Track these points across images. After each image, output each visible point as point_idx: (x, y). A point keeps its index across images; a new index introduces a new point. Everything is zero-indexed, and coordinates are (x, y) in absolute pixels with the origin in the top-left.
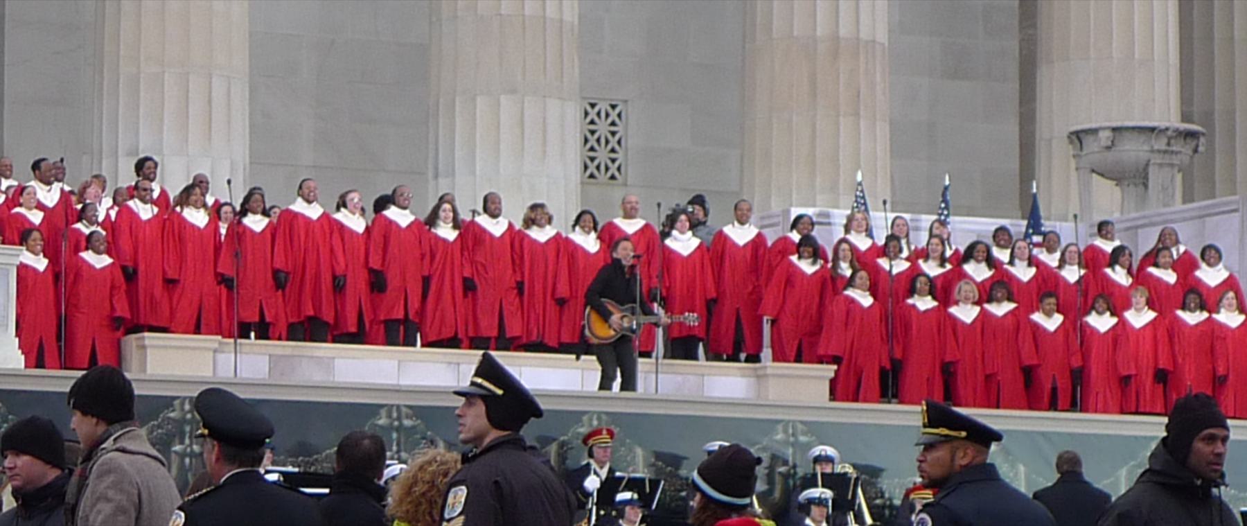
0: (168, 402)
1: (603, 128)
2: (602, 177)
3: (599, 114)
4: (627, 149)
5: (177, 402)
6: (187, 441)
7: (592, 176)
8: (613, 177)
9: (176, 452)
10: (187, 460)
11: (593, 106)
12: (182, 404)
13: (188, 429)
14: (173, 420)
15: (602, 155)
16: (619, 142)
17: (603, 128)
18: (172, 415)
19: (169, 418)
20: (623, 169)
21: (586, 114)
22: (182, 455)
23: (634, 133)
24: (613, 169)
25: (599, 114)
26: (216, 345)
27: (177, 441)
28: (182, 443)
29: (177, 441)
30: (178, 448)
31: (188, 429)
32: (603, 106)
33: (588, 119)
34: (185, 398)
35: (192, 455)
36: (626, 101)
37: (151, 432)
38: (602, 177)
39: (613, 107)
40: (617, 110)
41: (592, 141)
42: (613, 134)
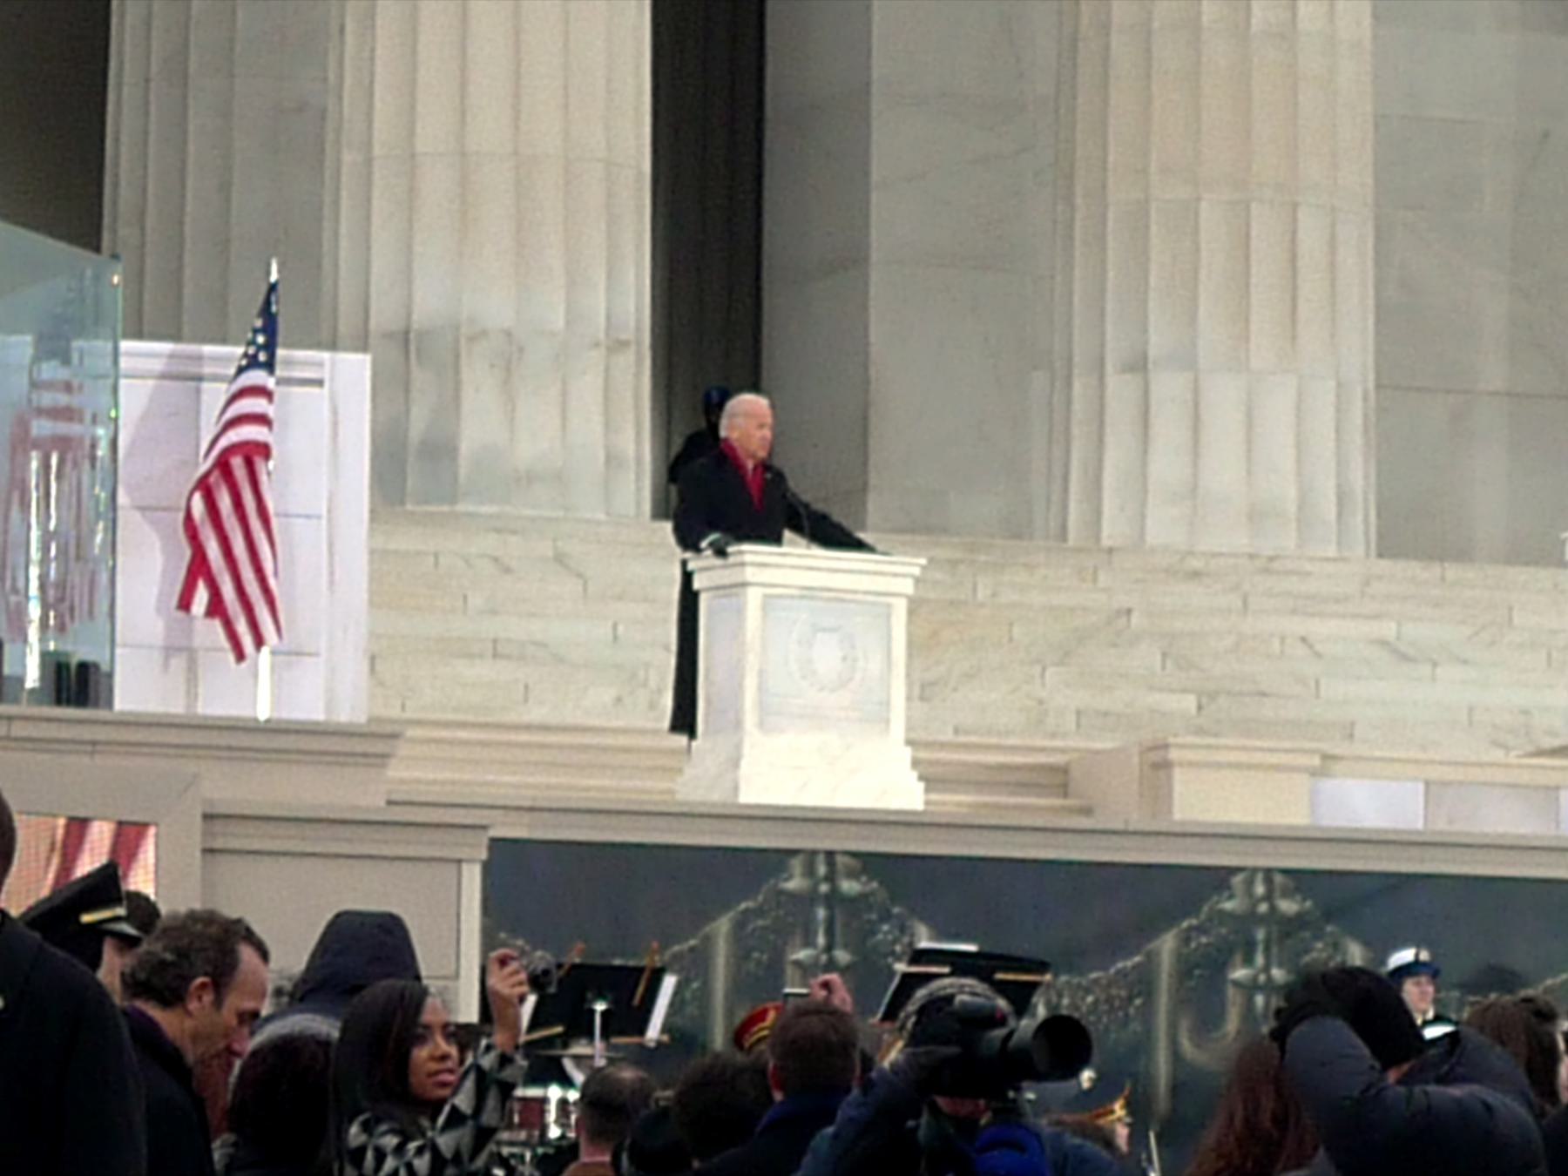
0: (1219, 878)
5: (1237, 880)
6: (1260, 960)
9: (1236, 984)
10: (1260, 1000)
12: (1250, 883)
13: (1260, 935)
14: (1231, 915)
18: (1228, 906)
19: (1222, 913)
22: (1250, 988)
26: (1316, 761)
27: (1238, 958)
28: (1248, 960)
29: (1238, 958)
30: (1240, 973)
31: (1260, 935)
34: (1255, 870)
35: (1269, 987)
37: (1186, 940)
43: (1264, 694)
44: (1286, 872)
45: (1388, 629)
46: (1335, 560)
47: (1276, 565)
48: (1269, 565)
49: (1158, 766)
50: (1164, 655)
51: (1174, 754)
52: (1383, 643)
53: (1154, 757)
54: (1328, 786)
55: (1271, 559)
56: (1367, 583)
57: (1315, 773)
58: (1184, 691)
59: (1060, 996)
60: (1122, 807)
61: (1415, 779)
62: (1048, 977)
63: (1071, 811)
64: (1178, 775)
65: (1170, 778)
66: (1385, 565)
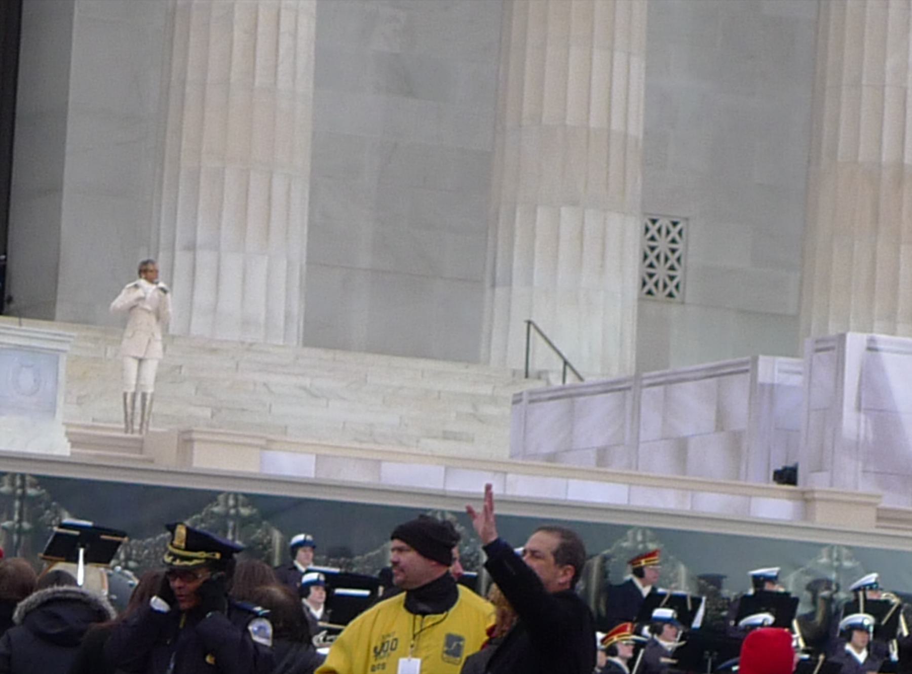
1: (663, 245)
2: (661, 294)
3: (659, 231)
4: (686, 267)
7: (650, 293)
8: (671, 295)
11: (654, 221)
15: (661, 272)
16: (678, 260)
17: (663, 245)
20: (681, 286)
21: (647, 230)
23: (694, 251)
24: (671, 286)
25: (659, 231)
32: (664, 223)
33: (649, 235)
36: (687, 219)
38: (661, 294)
39: (675, 224)
40: (679, 227)
41: (652, 258)
42: (673, 251)
43: (243, 410)
44: (245, 495)
45: (307, 382)
46: (283, 347)
47: (254, 347)
48: (250, 347)
49: (186, 441)
50: (197, 389)
51: (195, 436)
52: (304, 388)
53: (186, 437)
54: (269, 454)
55: (251, 344)
56: (297, 358)
57: (263, 448)
58: (207, 406)
59: (131, 550)
60: (168, 459)
61: (311, 453)
62: (126, 539)
63: (144, 461)
64: (196, 446)
65: (192, 448)
66: (306, 351)
